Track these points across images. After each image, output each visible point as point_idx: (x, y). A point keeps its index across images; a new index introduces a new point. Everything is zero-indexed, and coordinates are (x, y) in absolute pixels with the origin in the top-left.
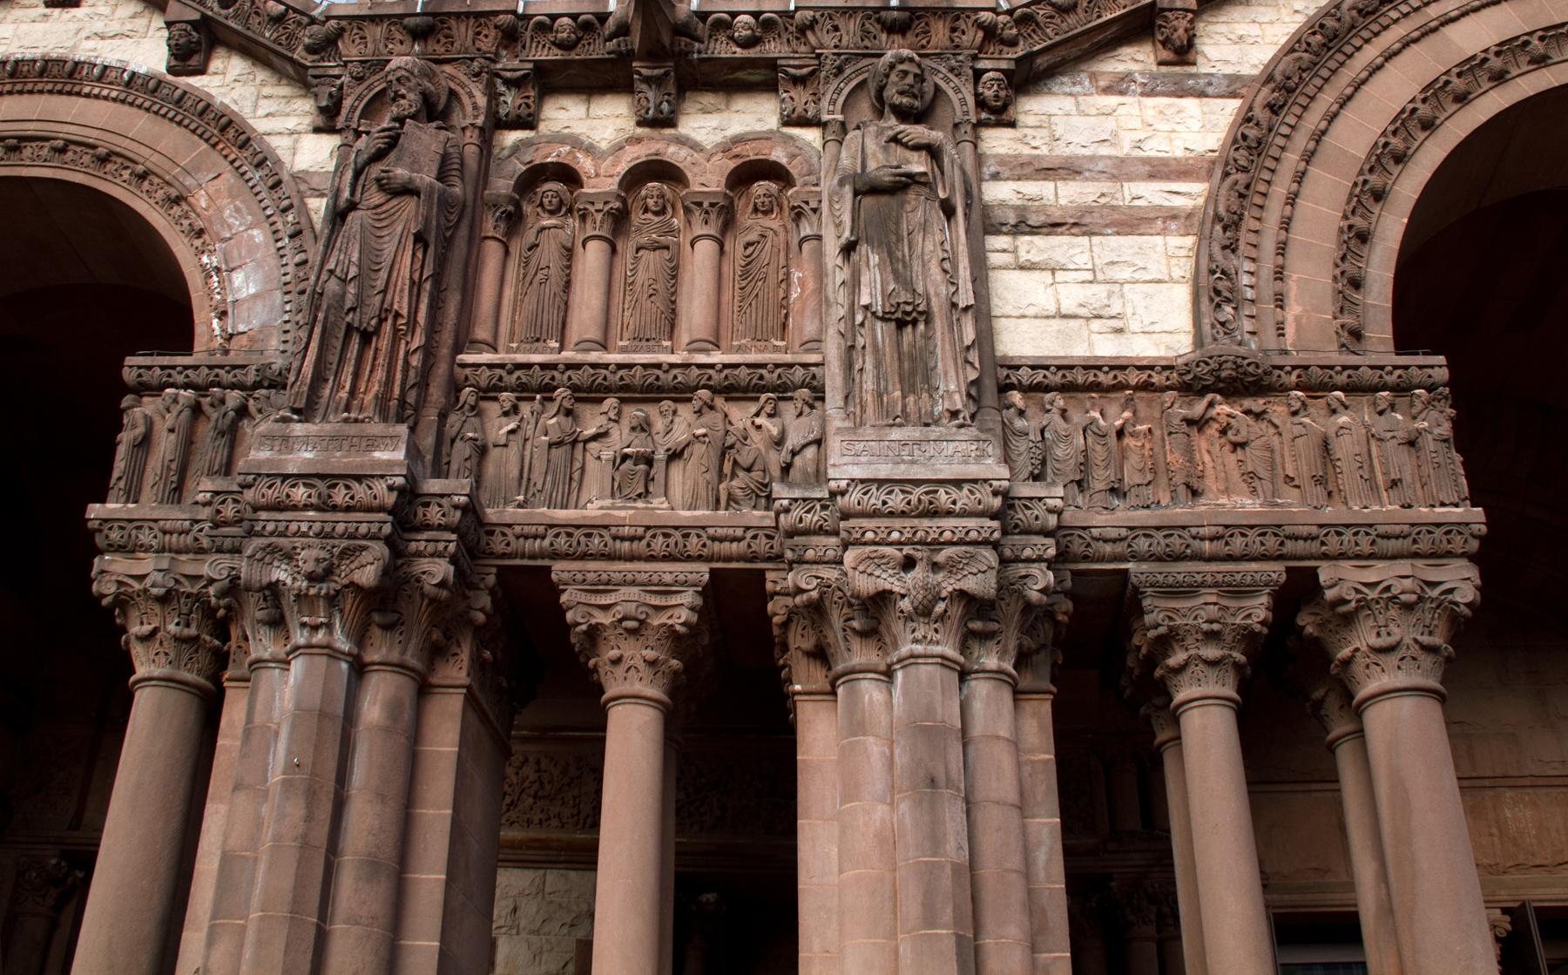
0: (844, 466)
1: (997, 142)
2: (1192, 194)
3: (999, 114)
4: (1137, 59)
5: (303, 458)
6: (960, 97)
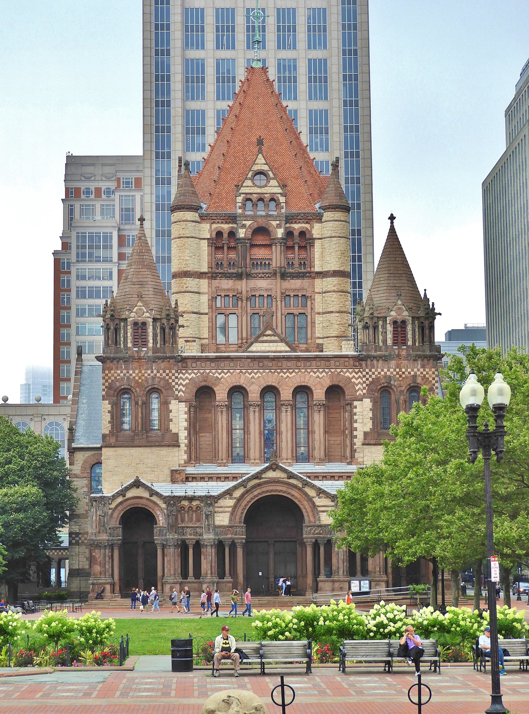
0: (205, 537)
1: (216, 505)
2: (230, 509)
3: (215, 503)
4: (228, 496)
5: (171, 537)
6: (213, 503)
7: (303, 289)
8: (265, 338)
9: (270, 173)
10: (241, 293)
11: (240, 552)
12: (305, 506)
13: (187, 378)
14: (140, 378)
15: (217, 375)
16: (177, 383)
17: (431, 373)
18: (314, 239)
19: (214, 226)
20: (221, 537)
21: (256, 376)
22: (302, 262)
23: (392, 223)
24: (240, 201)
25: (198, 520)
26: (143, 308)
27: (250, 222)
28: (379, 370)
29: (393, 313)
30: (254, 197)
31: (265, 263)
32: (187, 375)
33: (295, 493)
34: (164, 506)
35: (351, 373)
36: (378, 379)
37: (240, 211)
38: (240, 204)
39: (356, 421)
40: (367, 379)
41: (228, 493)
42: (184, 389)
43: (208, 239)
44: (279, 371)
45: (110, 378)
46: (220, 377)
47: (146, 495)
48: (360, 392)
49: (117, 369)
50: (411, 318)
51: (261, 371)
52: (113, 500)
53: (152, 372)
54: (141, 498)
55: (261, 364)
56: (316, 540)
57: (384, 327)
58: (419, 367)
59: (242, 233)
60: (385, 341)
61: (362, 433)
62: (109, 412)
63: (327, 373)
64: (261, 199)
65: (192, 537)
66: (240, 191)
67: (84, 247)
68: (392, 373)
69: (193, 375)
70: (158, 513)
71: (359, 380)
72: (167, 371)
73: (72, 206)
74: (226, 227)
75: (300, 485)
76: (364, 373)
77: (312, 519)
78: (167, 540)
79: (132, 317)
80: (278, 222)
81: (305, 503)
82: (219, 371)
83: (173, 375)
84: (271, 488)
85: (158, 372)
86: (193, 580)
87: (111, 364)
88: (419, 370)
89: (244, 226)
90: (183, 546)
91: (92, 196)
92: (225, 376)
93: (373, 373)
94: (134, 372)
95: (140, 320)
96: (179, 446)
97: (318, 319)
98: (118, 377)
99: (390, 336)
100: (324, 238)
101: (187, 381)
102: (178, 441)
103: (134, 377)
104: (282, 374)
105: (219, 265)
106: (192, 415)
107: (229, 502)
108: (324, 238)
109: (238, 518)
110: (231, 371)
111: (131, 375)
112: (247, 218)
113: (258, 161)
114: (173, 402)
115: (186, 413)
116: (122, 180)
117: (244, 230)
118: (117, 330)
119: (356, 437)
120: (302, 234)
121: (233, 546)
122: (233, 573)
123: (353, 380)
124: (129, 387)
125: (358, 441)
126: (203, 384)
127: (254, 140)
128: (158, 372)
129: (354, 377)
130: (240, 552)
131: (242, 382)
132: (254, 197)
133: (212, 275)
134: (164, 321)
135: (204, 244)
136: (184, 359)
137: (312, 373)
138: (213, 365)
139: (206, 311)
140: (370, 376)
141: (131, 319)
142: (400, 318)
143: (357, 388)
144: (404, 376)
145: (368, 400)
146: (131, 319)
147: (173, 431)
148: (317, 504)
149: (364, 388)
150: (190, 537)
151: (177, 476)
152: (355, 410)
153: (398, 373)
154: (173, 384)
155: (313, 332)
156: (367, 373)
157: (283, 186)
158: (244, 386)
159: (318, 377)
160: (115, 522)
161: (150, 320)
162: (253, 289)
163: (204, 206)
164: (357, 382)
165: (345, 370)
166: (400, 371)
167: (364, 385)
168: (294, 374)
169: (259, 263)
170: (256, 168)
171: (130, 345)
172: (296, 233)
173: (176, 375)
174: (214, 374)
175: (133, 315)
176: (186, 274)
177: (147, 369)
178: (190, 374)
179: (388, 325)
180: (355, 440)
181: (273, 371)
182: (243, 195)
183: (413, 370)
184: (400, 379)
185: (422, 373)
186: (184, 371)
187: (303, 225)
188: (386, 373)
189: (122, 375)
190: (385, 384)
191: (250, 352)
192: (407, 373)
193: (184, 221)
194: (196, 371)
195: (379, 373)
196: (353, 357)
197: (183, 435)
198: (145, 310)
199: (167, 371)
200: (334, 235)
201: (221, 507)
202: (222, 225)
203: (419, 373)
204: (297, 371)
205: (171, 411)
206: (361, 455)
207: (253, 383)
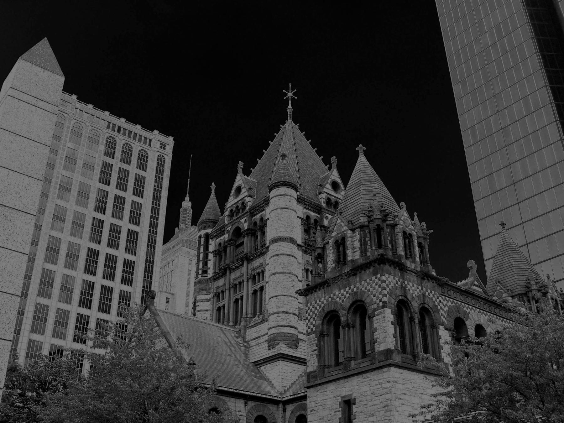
19: (305, 210)
26: (409, 219)
42: (446, 316)
43: (302, 219)
53: (422, 289)
87: (389, 268)
89: (327, 218)
98: (397, 285)
103: (409, 290)
124: (406, 299)
141: (401, 227)
193: (290, 196)
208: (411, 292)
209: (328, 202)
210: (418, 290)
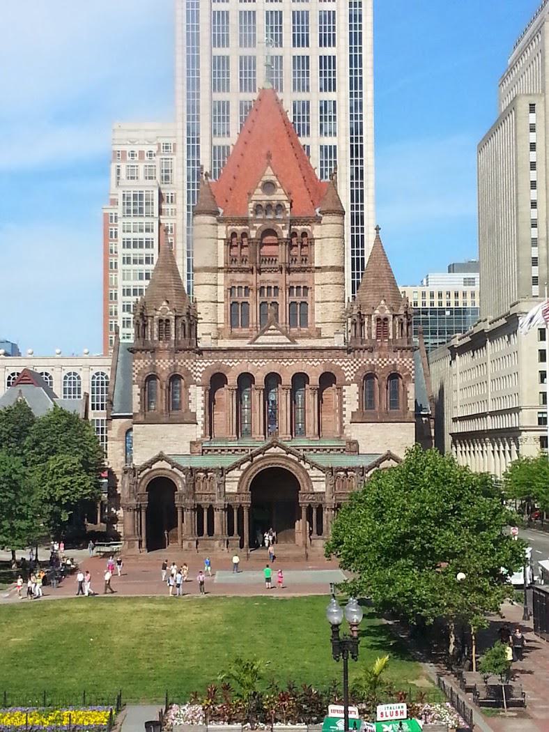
0: (217, 502)
1: (227, 475)
2: (238, 479)
7: (305, 282)
8: (269, 332)
9: (277, 183)
10: (252, 285)
11: (246, 513)
12: (300, 477)
13: (203, 366)
14: (164, 366)
15: (228, 363)
16: (195, 371)
17: (408, 362)
18: (314, 239)
19: (229, 228)
20: (230, 502)
21: (261, 365)
22: (304, 258)
23: (378, 233)
24: (252, 206)
25: (212, 488)
27: (260, 225)
28: (365, 360)
29: (377, 312)
30: (264, 204)
31: (272, 259)
32: (203, 364)
33: (292, 465)
34: (183, 476)
35: (341, 362)
36: (364, 367)
37: (251, 215)
38: (252, 210)
39: (345, 403)
40: (355, 367)
41: (237, 466)
42: (201, 375)
43: (224, 239)
44: (280, 360)
45: (139, 366)
46: (231, 365)
47: (169, 467)
48: (348, 378)
49: (145, 358)
50: (392, 316)
51: (266, 360)
52: (141, 472)
53: (174, 361)
54: (164, 469)
55: (265, 355)
56: (310, 505)
57: (369, 323)
58: (399, 356)
59: (253, 234)
60: (370, 336)
61: (351, 413)
62: (138, 394)
63: (321, 362)
64: (269, 206)
65: (206, 502)
66: (252, 199)
67: (129, 204)
68: (375, 362)
69: (208, 364)
70: (179, 482)
71: (348, 368)
72: (187, 361)
73: (119, 166)
74: (239, 229)
75: (296, 459)
76: (352, 362)
77: (307, 488)
78: (186, 504)
79: (158, 315)
80: (284, 225)
81: (301, 474)
82: (231, 360)
83: (192, 363)
84: (272, 462)
85: (179, 361)
86: (207, 537)
88: (398, 360)
90: (198, 509)
91: (136, 158)
92: (236, 365)
93: (360, 363)
94: (159, 361)
95: (165, 317)
96: (197, 424)
97: (317, 306)
98: (146, 366)
99: (374, 331)
100: (323, 238)
101: (204, 369)
102: (196, 419)
104: (283, 363)
105: (233, 260)
106: (207, 397)
107: (237, 473)
108: (323, 238)
109: (244, 488)
110: (241, 360)
111: (156, 363)
112: (258, 221)
113: (267, 172)
114: (191, 386)
115: (202, 395)
116: (162, 145)
117: (255, 232)
118: (145, 326)
119: (345, 416)
120: (304, 234)
121: (240, 510)
122: (241, 533)
123: (343, 368)
125: (347, 420)
126: (217, 371)
127: (264, 152)
128: (179, 361)
129: (343, 365)
130: (246, 513)
131: (249, 370)
132: (264, 204)
133: (228, 270)
134: (185, 318)
135: (221, 244)
136: (200, 352)
137: (308, 362)
138: (225, 355)
139: (223, 300)
140: (357, 365)
141: (157, 317)
142: (382, 316)
143: (346, 375)
144: (385, 365)
145: (356, 385)
146: (157, 317)
147: (192, 411)
148: (310, 475)
149: (352, 375)
150: (205, 502)
151: (195, 448)
152: (344, 394)
153: (380, 362)
154: (192, 371)
155: (313, 318)
156: (355, 363)
157: (289, 194)
158: (251, 373)
159: (313, 365)
160: (142, 489)
161: (173, 318)
162: (262, 281)
163: (221, 211)
164: (346, 370)
165: (336, 360)
166: (383, 360)
167: (352, 372)
168: (293, 363)
169: (267, 259)
170: (265, 178)
171: (156, 338)
172: (299, 234)
173: (195, 363)
174: (226, 363)
175: (158, 313)
176: (207, 269)
177: (170, 359)
178: (206, 363)
179: (373, 322)
180: (344, 419)
181: (275, 360)
182: (254, 202)
183: (393, 360)
184: (383, 367)
185: (400, 362)
186: (201, 361)
187: (305, 227)
188: (370, 362)
189: (149, 363)
190: (370, 372)
191: (258, 344)
192: (388, 362)
194: (211, 361)
195: (365, 362)
196: (343, 349)
197: (200, 414)
198: (169, 309)
199: (187, 361)
200: (331, 235)
201: (230, 477)
202: (237, 227)
203: (398, 362)
204: (295, 360)
205: (190, 394)
206: (349, 431)
207: (258, 370)
208: (162, 366)
209: (258, 209)
210: (169, 363)
